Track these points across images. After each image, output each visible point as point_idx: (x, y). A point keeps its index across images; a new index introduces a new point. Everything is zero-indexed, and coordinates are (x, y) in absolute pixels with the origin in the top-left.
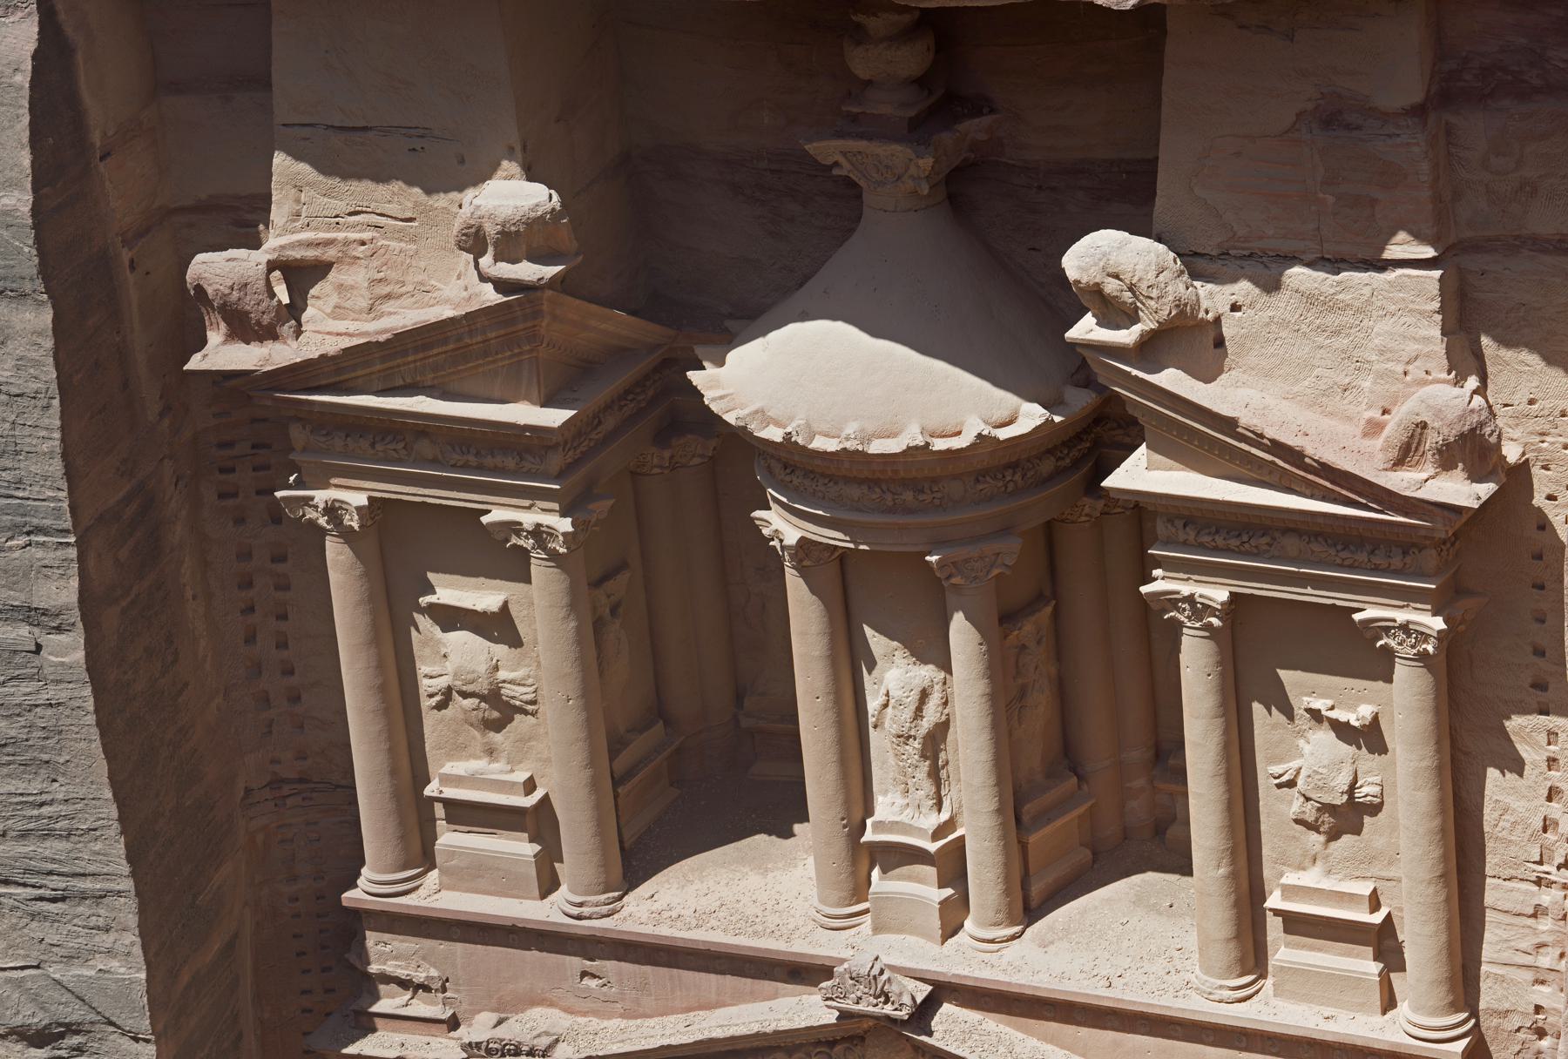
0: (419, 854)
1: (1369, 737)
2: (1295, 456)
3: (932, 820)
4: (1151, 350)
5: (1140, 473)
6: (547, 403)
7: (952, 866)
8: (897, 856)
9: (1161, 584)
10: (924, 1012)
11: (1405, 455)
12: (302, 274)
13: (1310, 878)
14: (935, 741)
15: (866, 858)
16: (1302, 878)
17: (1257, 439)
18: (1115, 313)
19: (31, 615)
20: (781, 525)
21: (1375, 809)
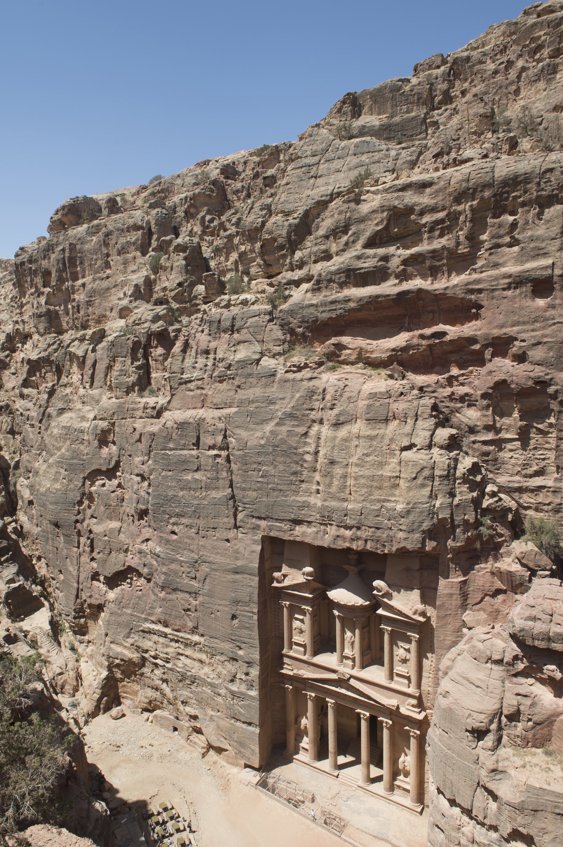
0: (291, 648)
1: (408, 651)
2: (400, 612)
3: (352, 653)
4: (383, 596)
5: (380, 611)
6: (310, 594)
7: (354, 660)
8: (347, 658)
9: (382, 626)
10: (349, 679)
11: (415, 613)
12: (285, 576)
13: (400, 668)
14: (353, 643)
15: (343, 657)
16: (399, 668)
17: (396, 609)
18: (379, 591)
19: (253, 612)
20: (336, 613)
21: (408, 660)
